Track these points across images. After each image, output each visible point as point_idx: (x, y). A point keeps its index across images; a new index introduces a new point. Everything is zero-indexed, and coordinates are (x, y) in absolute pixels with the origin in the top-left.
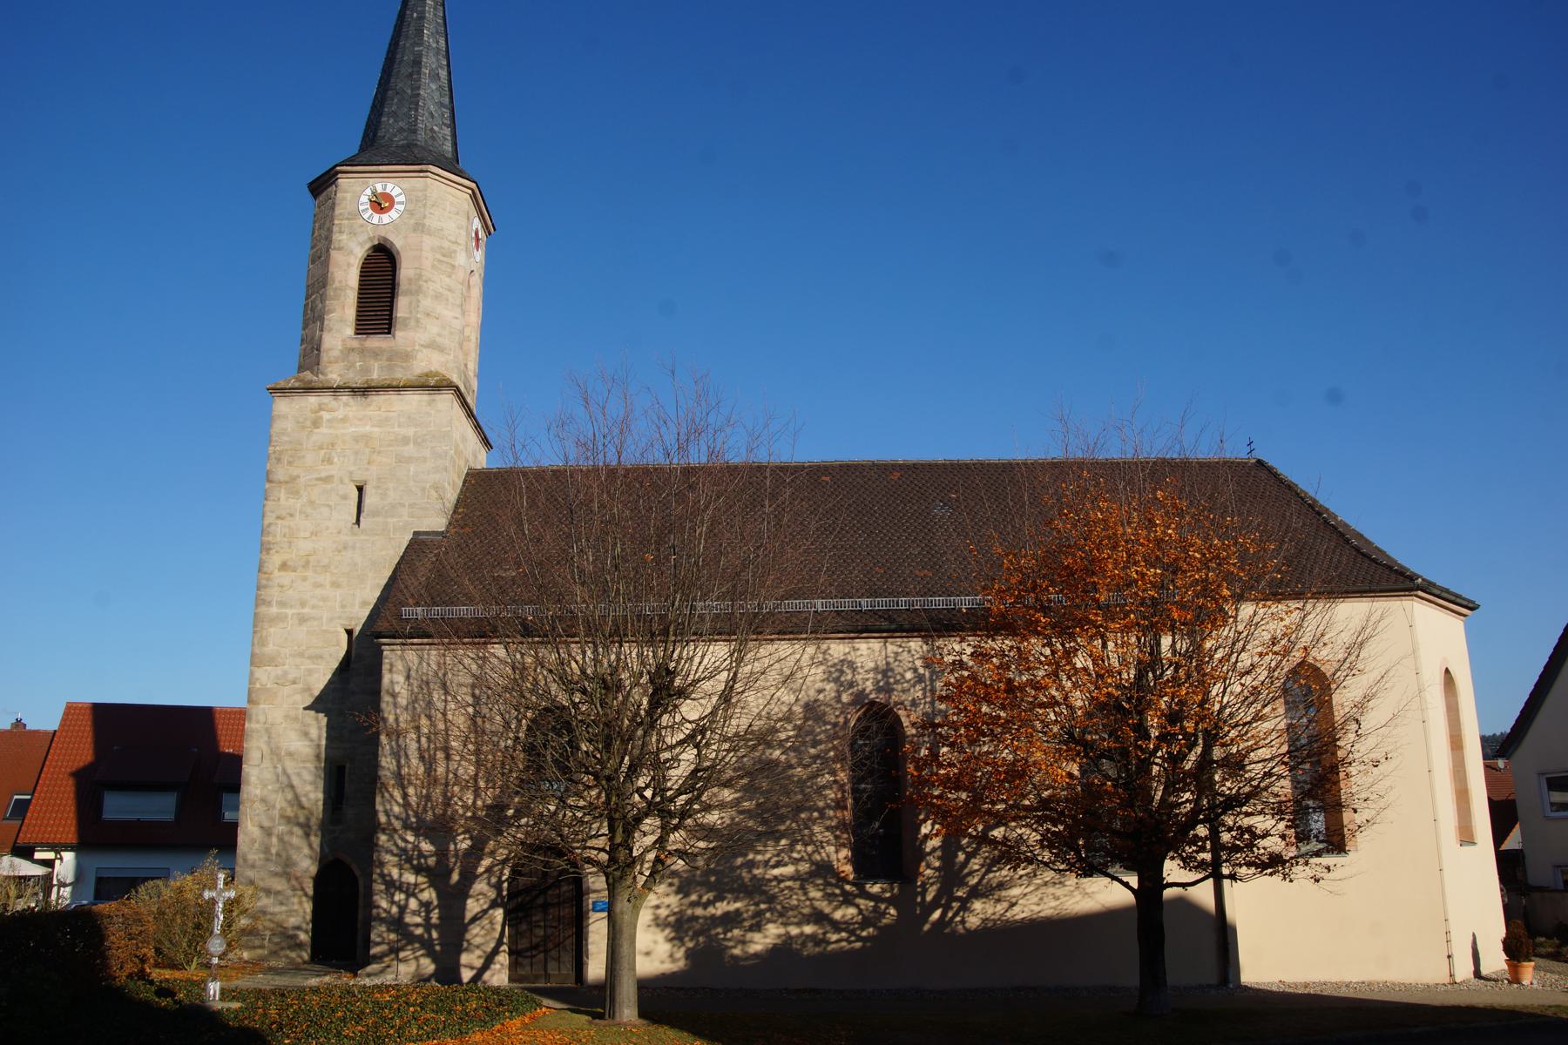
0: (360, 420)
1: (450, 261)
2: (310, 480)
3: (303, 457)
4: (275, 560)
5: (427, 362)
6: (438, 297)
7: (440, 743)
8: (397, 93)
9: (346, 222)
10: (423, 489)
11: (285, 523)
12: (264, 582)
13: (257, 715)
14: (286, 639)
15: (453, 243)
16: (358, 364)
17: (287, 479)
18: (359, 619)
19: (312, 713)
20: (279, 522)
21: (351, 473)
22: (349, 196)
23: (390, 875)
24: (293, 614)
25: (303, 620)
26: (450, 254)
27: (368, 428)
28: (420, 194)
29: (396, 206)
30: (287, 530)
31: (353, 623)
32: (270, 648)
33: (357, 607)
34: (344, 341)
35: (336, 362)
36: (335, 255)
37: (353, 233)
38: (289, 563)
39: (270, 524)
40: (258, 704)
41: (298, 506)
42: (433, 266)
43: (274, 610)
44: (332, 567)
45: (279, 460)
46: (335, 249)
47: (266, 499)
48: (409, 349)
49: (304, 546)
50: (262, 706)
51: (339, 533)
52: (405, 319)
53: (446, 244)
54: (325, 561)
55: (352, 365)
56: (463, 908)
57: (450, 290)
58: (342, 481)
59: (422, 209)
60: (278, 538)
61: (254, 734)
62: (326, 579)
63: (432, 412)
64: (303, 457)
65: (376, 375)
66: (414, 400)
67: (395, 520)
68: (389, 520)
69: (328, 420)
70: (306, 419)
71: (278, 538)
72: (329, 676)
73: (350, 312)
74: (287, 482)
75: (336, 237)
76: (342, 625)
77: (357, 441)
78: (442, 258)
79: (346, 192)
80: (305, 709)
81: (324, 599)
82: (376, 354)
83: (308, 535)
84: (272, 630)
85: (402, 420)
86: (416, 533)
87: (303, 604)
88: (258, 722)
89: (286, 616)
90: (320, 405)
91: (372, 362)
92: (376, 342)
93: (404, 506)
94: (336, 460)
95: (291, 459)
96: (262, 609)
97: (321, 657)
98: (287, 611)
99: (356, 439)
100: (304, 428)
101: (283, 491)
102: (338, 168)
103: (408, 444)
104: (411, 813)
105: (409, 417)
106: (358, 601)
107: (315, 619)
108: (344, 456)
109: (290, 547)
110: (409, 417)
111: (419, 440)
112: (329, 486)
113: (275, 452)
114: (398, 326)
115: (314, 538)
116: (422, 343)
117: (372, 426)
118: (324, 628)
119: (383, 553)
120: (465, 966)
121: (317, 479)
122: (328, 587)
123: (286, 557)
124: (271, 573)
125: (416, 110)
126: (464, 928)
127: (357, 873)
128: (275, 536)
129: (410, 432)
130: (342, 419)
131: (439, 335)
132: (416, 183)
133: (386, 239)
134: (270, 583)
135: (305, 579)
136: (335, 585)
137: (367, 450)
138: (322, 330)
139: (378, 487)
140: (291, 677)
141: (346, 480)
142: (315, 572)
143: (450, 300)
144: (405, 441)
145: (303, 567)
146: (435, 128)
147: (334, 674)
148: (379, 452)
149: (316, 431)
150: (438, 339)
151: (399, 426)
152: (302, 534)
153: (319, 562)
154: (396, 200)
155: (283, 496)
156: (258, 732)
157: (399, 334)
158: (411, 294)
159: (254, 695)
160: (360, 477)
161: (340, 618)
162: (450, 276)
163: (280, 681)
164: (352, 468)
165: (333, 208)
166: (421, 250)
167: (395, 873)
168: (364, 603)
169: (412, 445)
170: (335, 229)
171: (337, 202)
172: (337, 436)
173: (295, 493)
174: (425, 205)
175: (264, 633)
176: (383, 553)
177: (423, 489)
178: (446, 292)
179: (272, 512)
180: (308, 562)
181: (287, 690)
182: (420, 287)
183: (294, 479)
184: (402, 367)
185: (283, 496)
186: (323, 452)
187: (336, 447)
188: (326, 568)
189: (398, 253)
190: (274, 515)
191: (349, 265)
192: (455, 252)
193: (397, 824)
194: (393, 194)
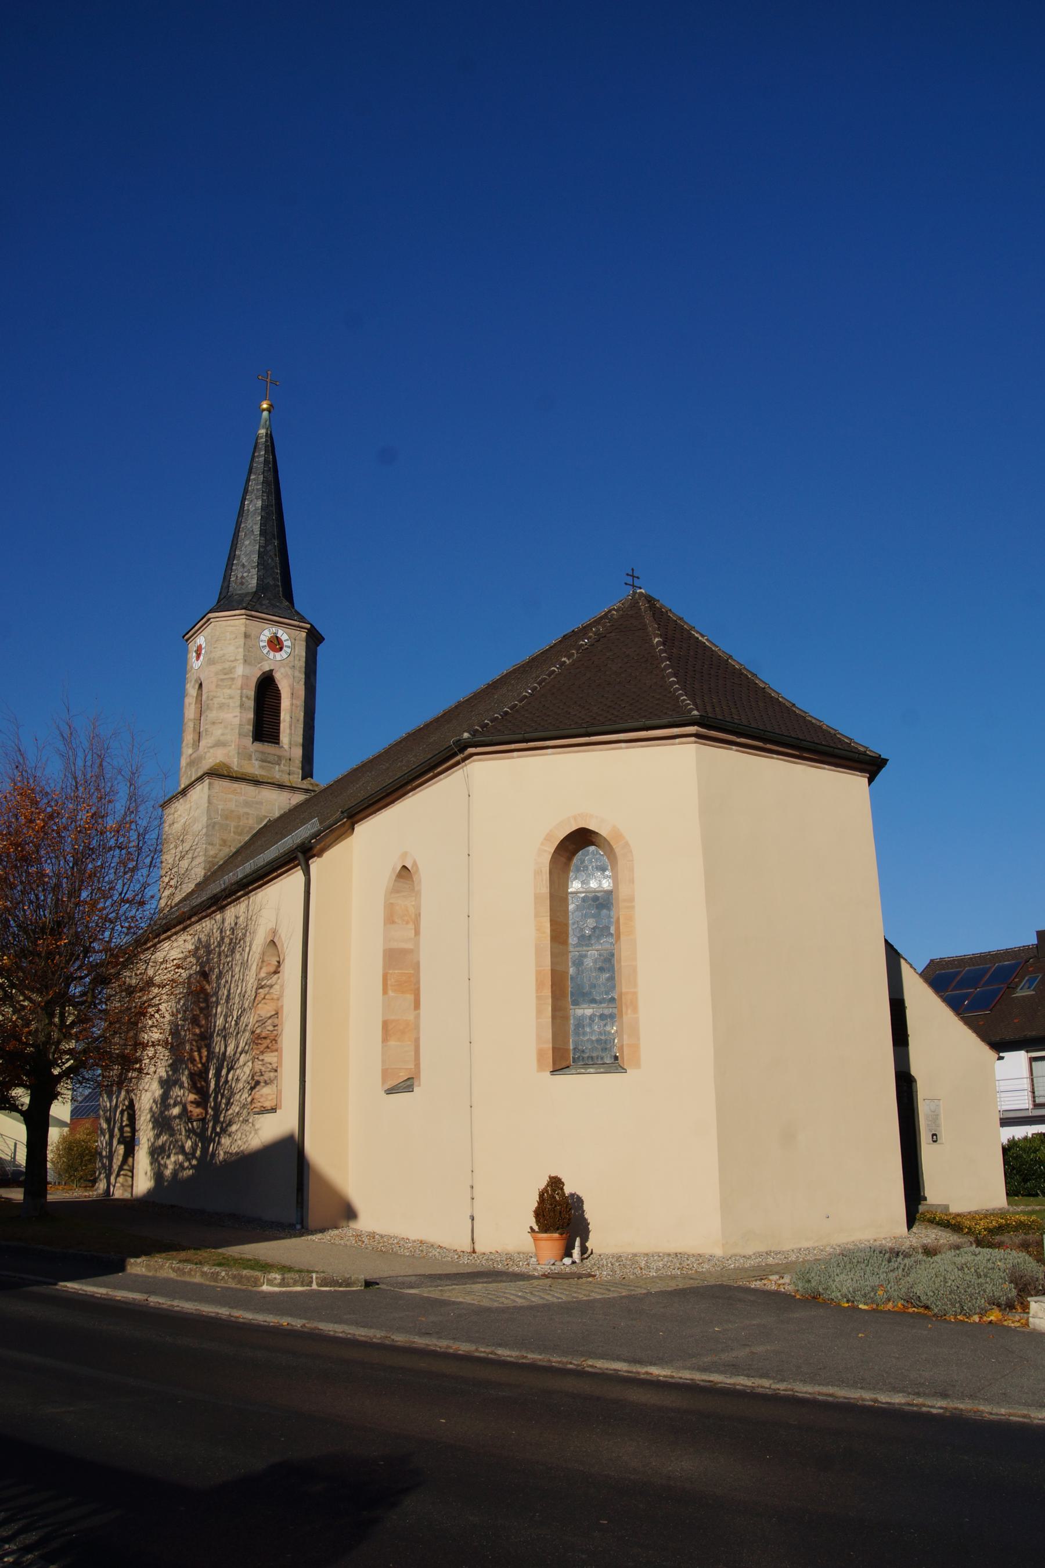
1: (231, 676)
5: (212, 758)
6: (221, 706)
15: (233, 661)
26: (231, 670)
42: (217, 686)
53: (227, 665)
57: (231, 698)
131: (223, 734)
143: (231, 704)
146: (245, 574)
150: (222, 738)
162: (230, 688)
192: (234, 667)
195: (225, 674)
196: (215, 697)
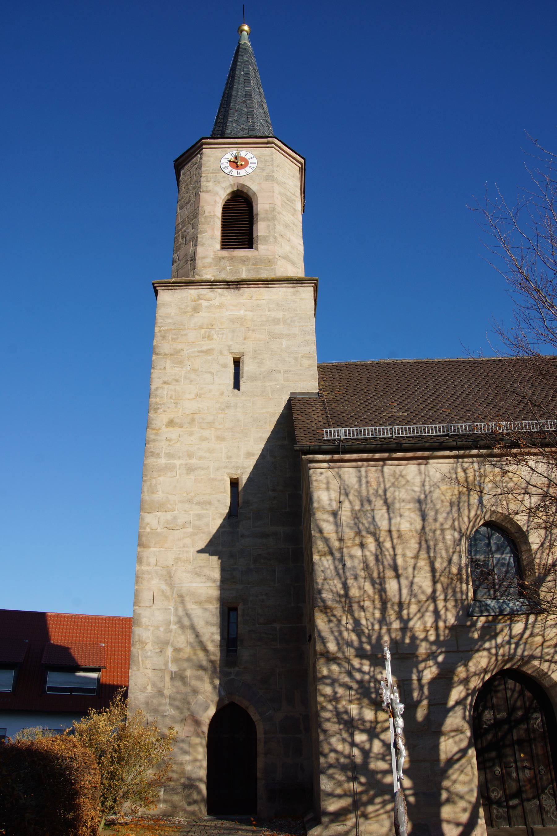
0: (234, 306)
1: (291, 205)
3: (186, 335)
6: (286, 226)
7: (388, 560)
8: (237, 111)
9: (212, 175)
10: (296, 359)
11: (171, 387)
13: (148, 557)
14: (175, 487)
16: (228, 268)
18: (244, 468)
19: (206, 556)
20: (166, 386)
21: (229, 347)
22: (212, 159)
23: (346, 712)
24: (181, 465)
25: (190, 469)
27: (242, 312)
28: (267, 158)
29: (249, 165)
31: (239, 472)
32: (159, 496)
34: (215, 252)
35: (210, 267)
36: (204, 196)
37: (217, 182)
38: (175, 420)
39: (157, 389)
40: (149, 547)
43: (163, 461)
45: (164, 337)
46: (203, 192)
48: (271, 257)
49: (189, 406)
50: (152, 549)
51: (222, 394)
52: (265, 237)
54: (210, 418)
55: (224, 268)
56: (436, 748)
58: (221, 353)
59: (271, 167)
61: (146, 576)
64: (186, 335)
67: (272, 383)
68: (268, 384)
69: (207, 307)
70: (187, 306)
72: (219, 521)
73: (218, 233)
74: (171, 355)
75: (203, 184)
76: (228, 474)
78: (287, 202)
79: (210, 156)
80: (200, 551)
81: (211, 451)
82: (243, 261)
84: (161, 479)
85: (271, 306)
86: (291, 394)
87: (190, 456)
88: (148, 565)
89: (174, 466)
90: (198, 296)
91: (240, 266)
93: (280, 372)
94: (215, 336)
95: (175, 337)
97: (210, 503)
98: (175, 462)
99: (233, 321)
100: (185, 312)
101: (168, 361)
102: (204, 141)
103: (278, 324)
104: (364, 639)
107: (202, 468)
109: (176, 407)
110: (278, 304)
111: (288, 321)
112: (210, 358)
114: (259, 242)
115: (198, 399)
116: (280, 254)
118: (212, 476)
119: (264, 411)
120: (448, 822)
121: (199, 352)
124: (159, 429)
125: (253, 119)
126: (443, 773)
127: (255, 717)
128: (162, 398)
129: (280, 315)
130: (218, 306)
132: (266, 151)
133: (243, 186)
134: (159, 438)
135: (191, 434)
136: (220, 438)
138: (196, 245)
139: (254, 358)
140: (180, 521)
141: (226, 352)
144: (276, 321)
145: (189, 423)
147: (224, 520)
148: (253, 331)
149: (196, 314)
150: (289, 255)
151: (269, 311)
152: (187, 396)
154: (250, 161)
155: (168, 365)
156: (149, 573)
157: (260, 247)
158: (268, 220)
159: (144, 539)
160: (237, 349)
161: (226, 467)
162: (293, 216)
163: (170, 527)
164: (231, 343)
165: (200, 168)
166: (273, 192)
167: (354, 710)
168: (249, 455)
169: (282, 324)
170: (202, 179)
171: (203, 162)
173: (181, 363)
174: (272, 165)
176: (264, 411)
178: (292, 225)
179: (159, 378)
180: (193, 420)
181: (178, 534)
182: (275, 216)
183: (178, 352)
184: (266, 270)
185: (168, 365)
186: (203, 331)
187: (214, 327)
188: (211, 424)
189: (255, 194)
190: (161, 381)
191: (215, 202)
193: (350, 652)
194: (247, 157)
195: (288, 201)
196: (281, 214)
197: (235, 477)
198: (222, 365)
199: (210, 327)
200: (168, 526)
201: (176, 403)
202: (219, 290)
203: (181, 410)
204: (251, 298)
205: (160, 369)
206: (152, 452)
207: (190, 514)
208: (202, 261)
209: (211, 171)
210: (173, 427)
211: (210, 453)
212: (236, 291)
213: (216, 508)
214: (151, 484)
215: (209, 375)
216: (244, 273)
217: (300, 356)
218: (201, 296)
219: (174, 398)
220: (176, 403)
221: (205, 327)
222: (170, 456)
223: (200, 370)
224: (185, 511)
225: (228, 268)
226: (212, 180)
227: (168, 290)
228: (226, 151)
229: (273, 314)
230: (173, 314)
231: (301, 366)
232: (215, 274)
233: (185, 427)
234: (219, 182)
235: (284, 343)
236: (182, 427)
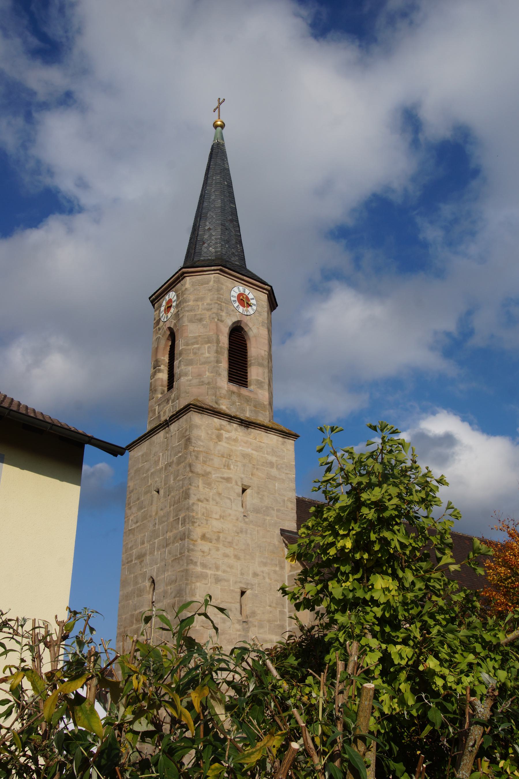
0: (245, 443)
2: (218, 477)
4: (197, 532)
9: (224, 304)
12: (191, 547)
16: (237, 404)
17: (203, 473)
20: (200, 503)
21: (242, 479)
24: (211, 574)
25: (218, 580)
27: (249, 451)
30: (205, 511)
33: (251, 575)
35: (225, 398)
41: (211, 494)
43: (199, 569)
44: (234, 544)
45: (197, 457)
47: (190, 484)
49: (216, 525)
51: (237, 519)
54: (229, 539)
55: (234, 403)
58: (236, 482)
60: (200, 516)
62: (230, 551)
63: (285, 449)
65: (248, 414)
66: (273, 439)
69: (226, 438)
71: (200, 516)
74: (203, 475)
77: (244, 458)
81: (231, 567)
83: (217, 517)
84: (198, 584)
85: (269, 450)
87: (217, 568)
90: (221, 425)
91: (245, 405)
92: (244, 391)
94: (232, 467)
95: (205, 459)
96: (191, 567)
99: (245, 456)
100: (211, 439)
101: (200, 480)
105: (273, 449)
106: (251, 572)
108: (237, 466)
109: (207, 524)
110: (273, 449)
112: (229, 485)
113: (194, 451)
115: (222, 520)
117: (253, 449)
118: (231, 588)
121: (222, 478)
122: (232, 557)
123: (205, 530)
124: (196, 541)
128: (197, 513)
129: (274, 459)
130: (234, 440)
137: (250, 465)
141: (240, 484)
142: (224, 545)
144: (271, 465)
149: (219, 443)
151: (268, 454)
152: (214, 516)
153: (226, 538)
161: (240, 582)
164: (243, 476)
169: (275, 468)
172: (232, 450)
173: (209, 484)
175: (193, 587)
177: (284, 501)
179: (195, 495)
180: (219, 538)
183: (206, 475)
184: (262, 413)
186: (224, 459)
187: (232, 458)
188: (230, 544)
197: (245, 590)
198: (237, 494)
199: (229, 457)
200: (204, 625)
201: (207, 520)
202: (235, 425)
203: (210, 527)
204: (255, 439)
205: (195, 486)
206: (191, 560)
207: (218, 617)
208: (219, 391)
209: (224, 300)
210: (205, 541)
211: (230, 568)
212: (246, 429)
213: (235, 614)
214: (191, 587)
215: (228, 501)
216: (248, 412)
217: (286, 499)
218: (222, 427)
219: (205, 515)
220: (207, 520)
221: (225, 456)
222: (204, 566)
223: (223, 495)
224: (215, 614)
225: (237, 404)
226: (225, 310)
227: (199, 413)
228: (234, 283)
229: (270, 458)
230: (202, 437)
231: (287, 508)
232: (229, 406)
233: (213, 542)
234: (230, 315)
235: (277, 484)
236: (211, 542)
